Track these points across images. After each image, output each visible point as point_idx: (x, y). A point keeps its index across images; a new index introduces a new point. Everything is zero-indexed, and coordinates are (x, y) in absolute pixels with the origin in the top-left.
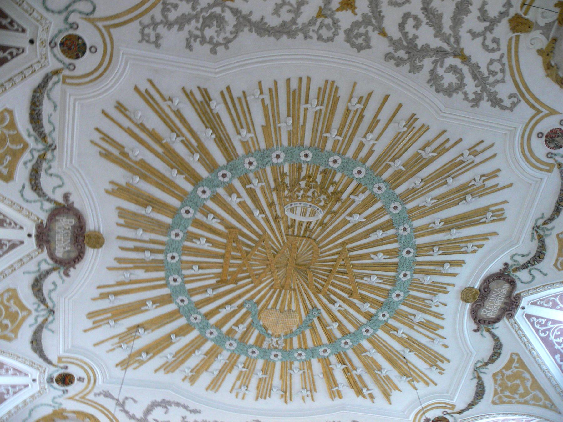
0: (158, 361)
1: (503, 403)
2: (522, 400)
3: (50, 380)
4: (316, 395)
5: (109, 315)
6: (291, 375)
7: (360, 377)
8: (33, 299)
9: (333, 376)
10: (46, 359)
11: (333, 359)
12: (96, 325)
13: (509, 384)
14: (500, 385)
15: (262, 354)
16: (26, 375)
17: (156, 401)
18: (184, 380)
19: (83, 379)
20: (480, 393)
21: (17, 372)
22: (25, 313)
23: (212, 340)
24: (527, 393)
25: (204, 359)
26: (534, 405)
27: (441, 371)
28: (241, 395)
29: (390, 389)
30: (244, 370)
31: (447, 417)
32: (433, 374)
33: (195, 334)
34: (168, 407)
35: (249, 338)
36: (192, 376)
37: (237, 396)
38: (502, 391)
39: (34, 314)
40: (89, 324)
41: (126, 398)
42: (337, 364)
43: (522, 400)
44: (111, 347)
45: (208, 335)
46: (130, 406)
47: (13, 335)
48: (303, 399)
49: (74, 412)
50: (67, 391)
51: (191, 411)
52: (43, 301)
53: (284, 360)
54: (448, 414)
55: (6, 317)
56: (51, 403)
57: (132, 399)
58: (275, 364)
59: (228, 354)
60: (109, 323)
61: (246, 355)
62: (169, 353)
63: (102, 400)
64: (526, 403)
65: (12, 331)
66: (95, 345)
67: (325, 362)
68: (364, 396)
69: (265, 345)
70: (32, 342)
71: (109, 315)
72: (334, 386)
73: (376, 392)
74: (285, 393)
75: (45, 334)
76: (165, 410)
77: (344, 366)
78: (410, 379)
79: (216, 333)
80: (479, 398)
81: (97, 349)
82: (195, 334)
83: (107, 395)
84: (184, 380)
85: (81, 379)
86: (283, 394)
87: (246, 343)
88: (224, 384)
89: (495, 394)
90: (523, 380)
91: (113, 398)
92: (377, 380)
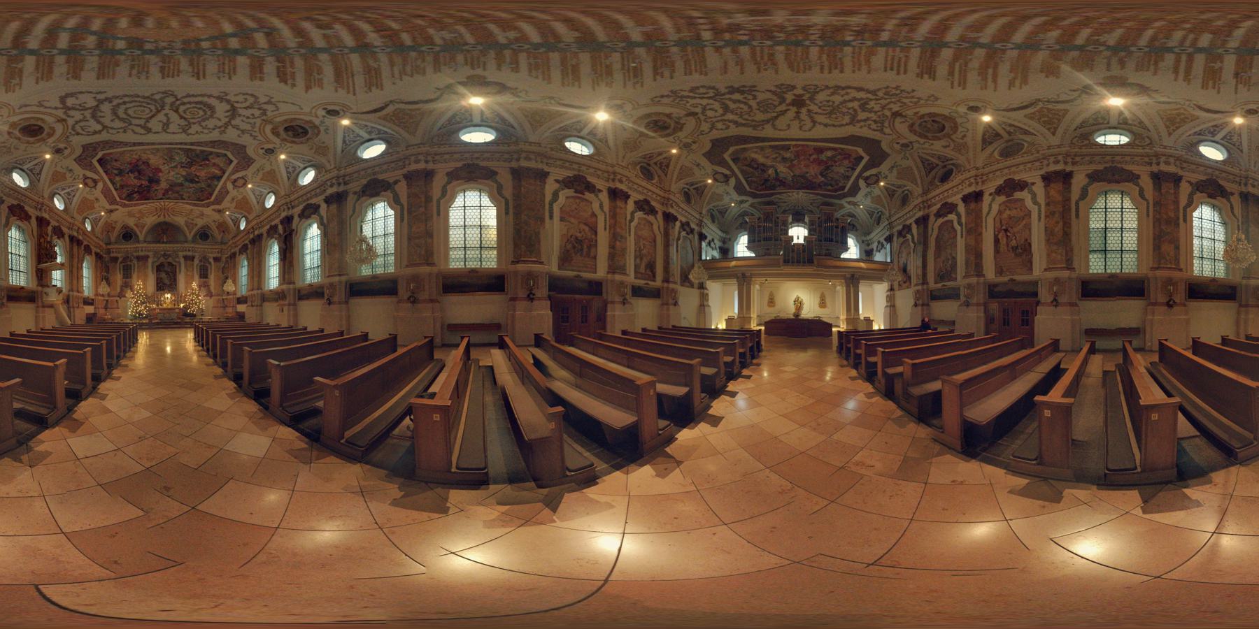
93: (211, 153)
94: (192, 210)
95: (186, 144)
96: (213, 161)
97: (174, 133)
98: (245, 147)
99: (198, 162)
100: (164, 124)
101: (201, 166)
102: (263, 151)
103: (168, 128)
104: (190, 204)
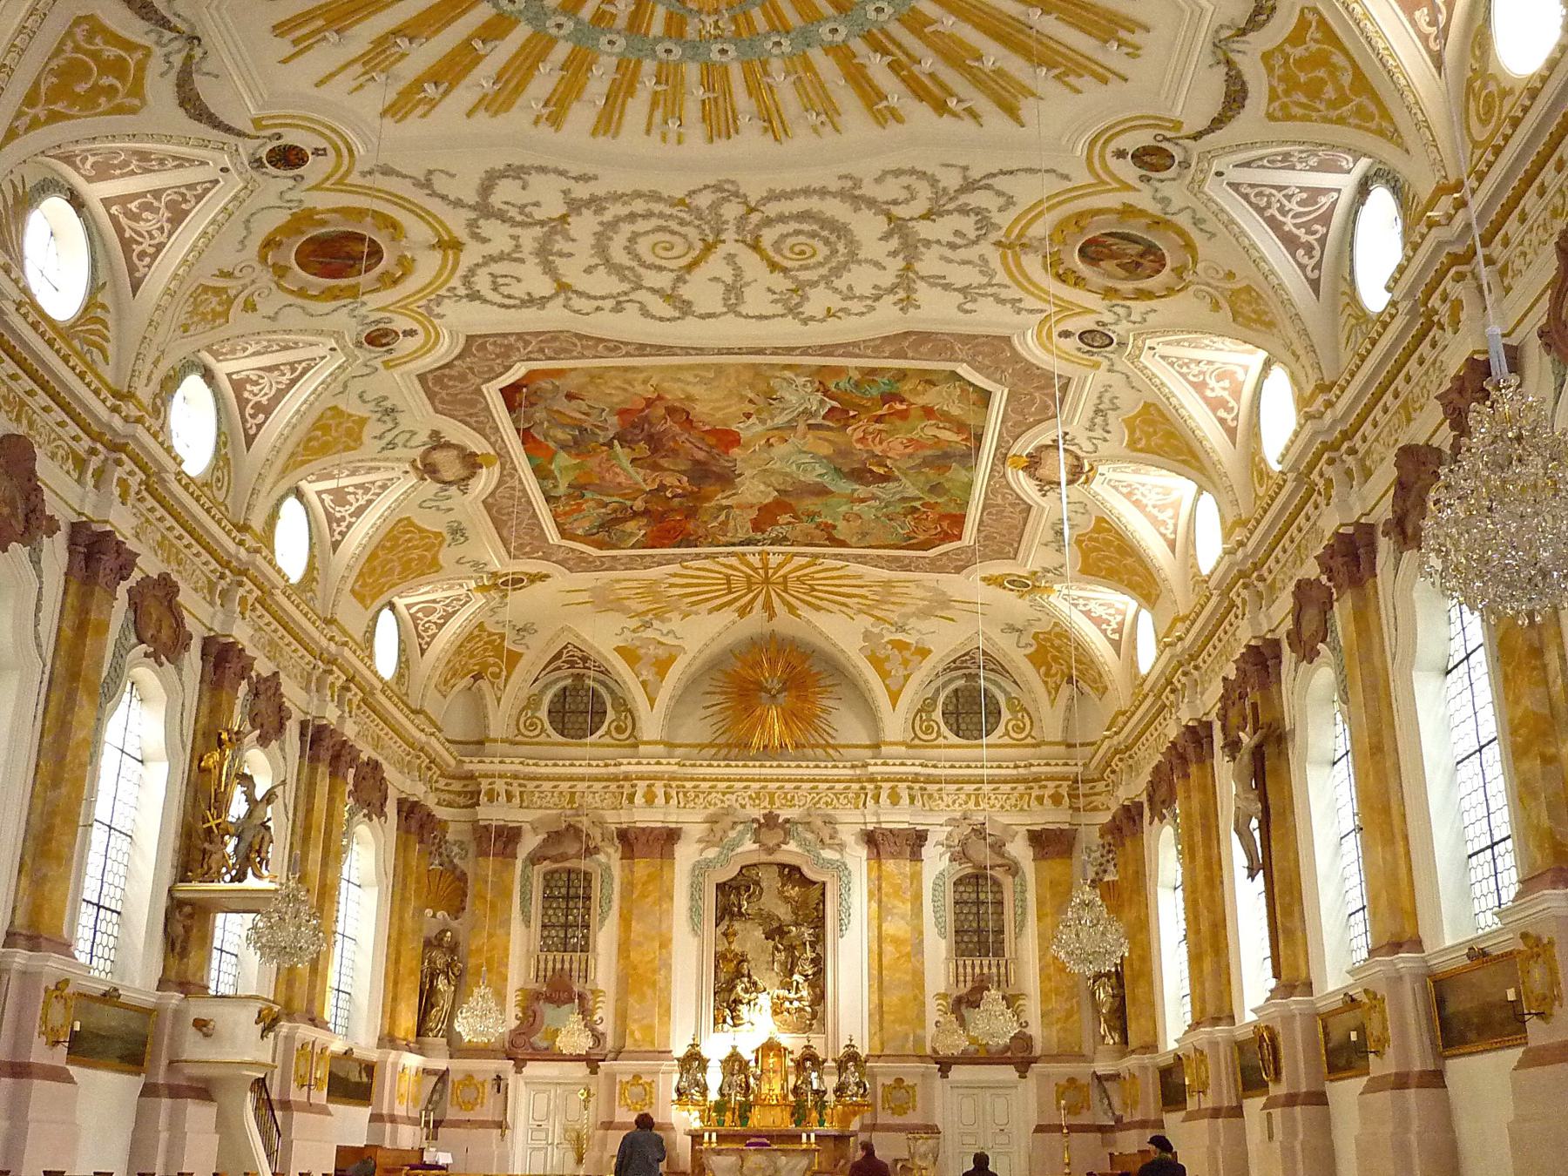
0: (465, 95)
1: (1290, 117)
2: (1334, 114)
3: (257, 163)
4: (840, 121)
5: (320, 23)
6: (770, 87)
7: (932, 76)
8: (146, 25)
9: (869, 81)
10: (228, 129)
11: (858, 45)
12: (302, 48)
13: (1303, 78)
14: (1280, 79)
15: (690, 53)
16: (202, 163)
17: (493, 169)
18: (536, 123)
19: (324, 150)
20: (1236, 96)
21: (181, 162)
22: (139, 55)
23: (566, 38)
24: (1347, 101)
25: (563, 78)
26: (1358, 127)
27: (1134, 52)
28: (672, 137)
29: (1015, 97)
30: (659, 88)
31: (1165, 145)
32: (1112, 56)
33: (522, 32)
34: (525, 177)
35: (649, 25)
36: (551, 112)
37: (664, 138)
38: (1287, 93)
39: (158, 52)
40: (285, 47)
41: (430, 172)
42: (871, 54)
43: (1334, 114)
44: (355, 84)
45: (554, 31)
46: (440, 184)
47: (137, 102)
48: (816, 130)
49: (335, 211)
50: (302, 178)
51: (576, 179)
52: (164, 23)
53: (746, 59)
54: (1168, 140)
55: (100, 75)
56: (279, 203)
57: (442, 171)
58: (726, 68)
59: (614, 60)
60: (325, 38)
61: (654, 59)
62: (482, 77)
63: (381, 182)
64: (1341, 120)
65: (129, 94)
66: (316, 85)
67: (842, 54)
68: (954, 115)
69: (691, 32)
70: (181, 105)
71: (320, 23)
72: (877, 100)
73: (982, 103)
74: (771, 122)
75: (201, 84)
76: (519, 183)
77: (890, 58)
78: (1057, 71)
79: (570, 25)
80: (1234, 106)
81: (325, 92)
82: (522, 32)
83: (387, 171)
84: (536, 123)
85: (316, 152)
86: (766, 124)
87: (646, 35)
88: (627, 119)
89: (1271, 100)
90: (1333, 70)
91: (405, 177)
92: (977, 80)
93: (903, 375)
94: (888, 584)
95: (805, 351)
96: (921, 401)
97: (761, 317)
98: (1007, 340)
99: (867, 409)
100: (729, 289)
101: (879, 419)
102: (1074, 342)
103: (740, 297)
104: (876, 562)
